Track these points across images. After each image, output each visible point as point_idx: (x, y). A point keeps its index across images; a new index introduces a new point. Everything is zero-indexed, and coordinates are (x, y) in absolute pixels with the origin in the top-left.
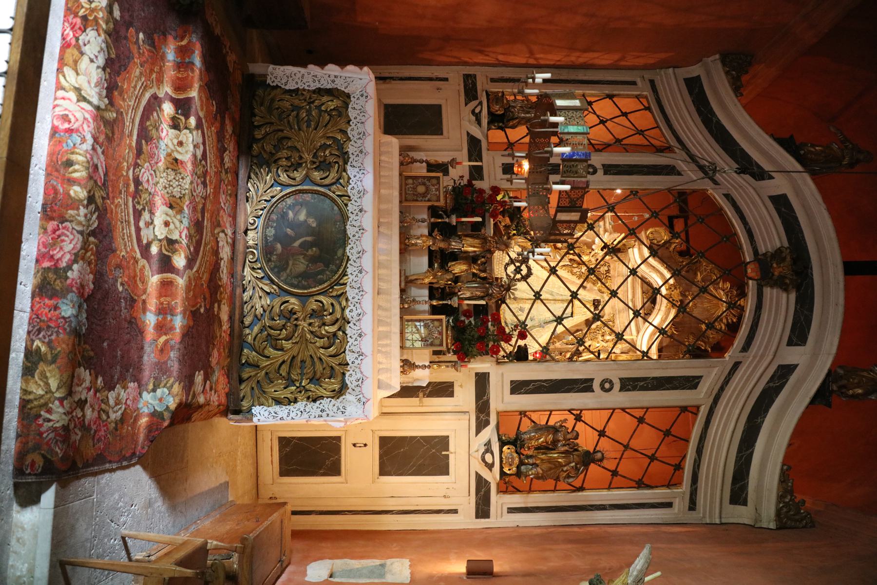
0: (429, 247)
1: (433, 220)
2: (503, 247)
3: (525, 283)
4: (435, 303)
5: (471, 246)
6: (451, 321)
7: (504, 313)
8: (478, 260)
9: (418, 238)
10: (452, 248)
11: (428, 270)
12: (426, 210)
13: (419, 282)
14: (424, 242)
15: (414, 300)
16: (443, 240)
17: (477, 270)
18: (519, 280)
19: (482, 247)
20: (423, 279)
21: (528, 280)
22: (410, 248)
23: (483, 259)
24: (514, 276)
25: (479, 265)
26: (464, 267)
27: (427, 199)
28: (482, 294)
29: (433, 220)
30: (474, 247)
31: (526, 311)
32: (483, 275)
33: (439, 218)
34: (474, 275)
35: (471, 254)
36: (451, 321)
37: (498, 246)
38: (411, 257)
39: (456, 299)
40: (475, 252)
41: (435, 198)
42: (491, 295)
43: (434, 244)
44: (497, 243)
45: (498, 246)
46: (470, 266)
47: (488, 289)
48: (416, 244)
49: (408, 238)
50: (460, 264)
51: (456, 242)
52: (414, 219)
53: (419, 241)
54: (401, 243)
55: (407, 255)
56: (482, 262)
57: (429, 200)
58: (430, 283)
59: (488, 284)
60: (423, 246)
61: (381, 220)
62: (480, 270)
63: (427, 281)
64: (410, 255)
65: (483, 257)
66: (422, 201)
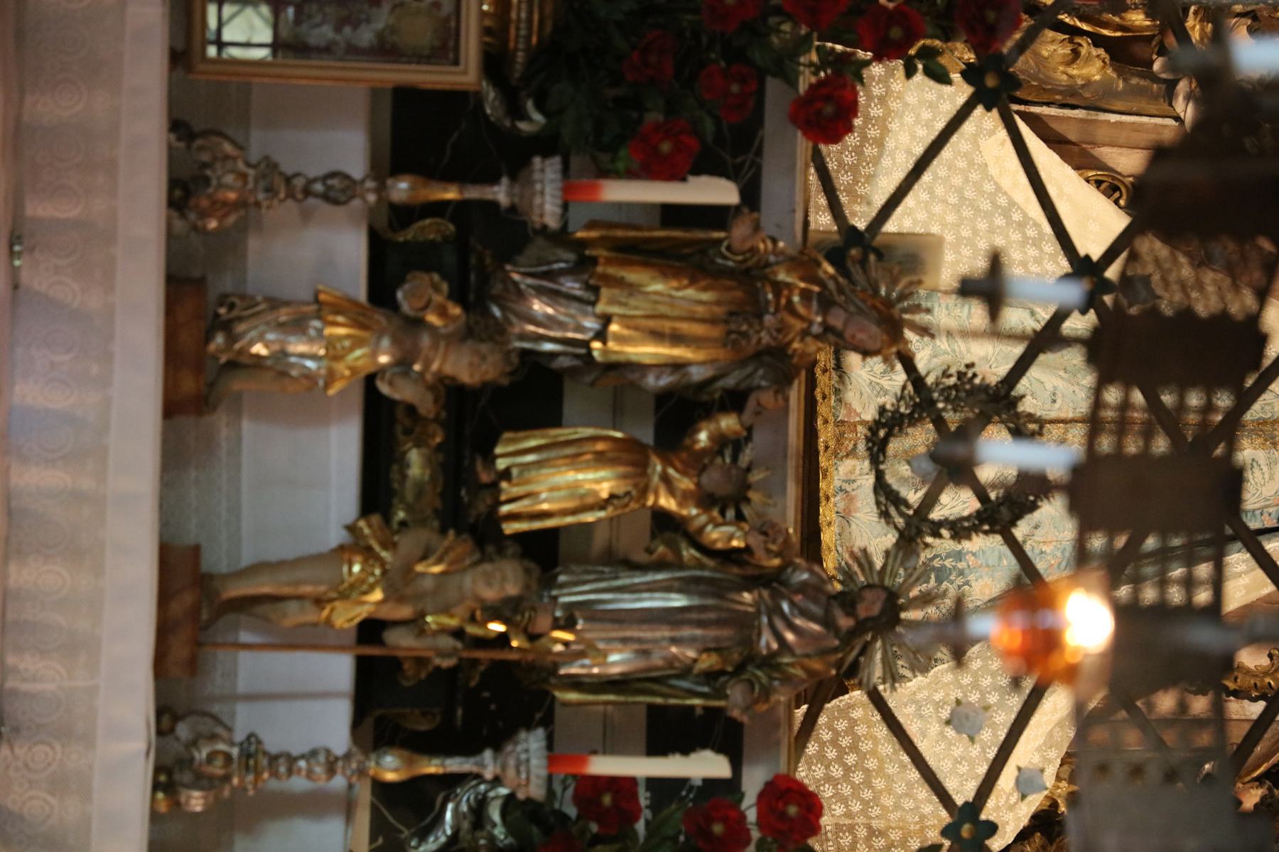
0: (370, 381)
1: (402, 188)
2: (871, 332)
3: (996, 541)
4: (391, 768)
5: (657, 336)
6: (495, 814)
7: (845, 516)
8: (690, 427)
9: (297, 326)
10: (524, 337)
11: (356, 546)
12: (359, 100)
13: (296, 615)
14: (335, 354)
15: (252, 752)
16: (468, 334)
17: (684, 498)
18: (960, 529)
19: (731, 339)
20: (319, 602)
21: (1020, 531)
22: (237, 384)
23: (728, 423)
24: (930, 500)
25: (697, 463)
26: (602, 482)
27: (366, 36)
28: (708, 662)
29: (402, 188)
30: (676, 339)
31: (992, 737)
32: (721, 535)
33: (447, 177)
34: (664, 522)
35: (651, 381)
36: (495, 814)
37: (837, 319)
38: (246, 425)
39: (532, 744)
40: (677, 366)
41: (420, 32)
42: (769, 662)
43: (403, 364)
44: (826, 303)
45: (837, 319)
46: (642, 467)
47: (745, 624)
48: (278, 366)
49: (226, 326)
50: (575, 454)
51: (554, 296)
52: (269, 167)
53: (298, 346)
54: (174, 357)
55: (221, 420)
56: (721, 442)
57: (386, 50)
58: (370, 630)
59: (751, 582)
60: (331, 377)
61: (37, 209)
62: (706, 500)
63: (346, 616)
64: (237, 412)
65: (735, 401)
66: (327, 50)
